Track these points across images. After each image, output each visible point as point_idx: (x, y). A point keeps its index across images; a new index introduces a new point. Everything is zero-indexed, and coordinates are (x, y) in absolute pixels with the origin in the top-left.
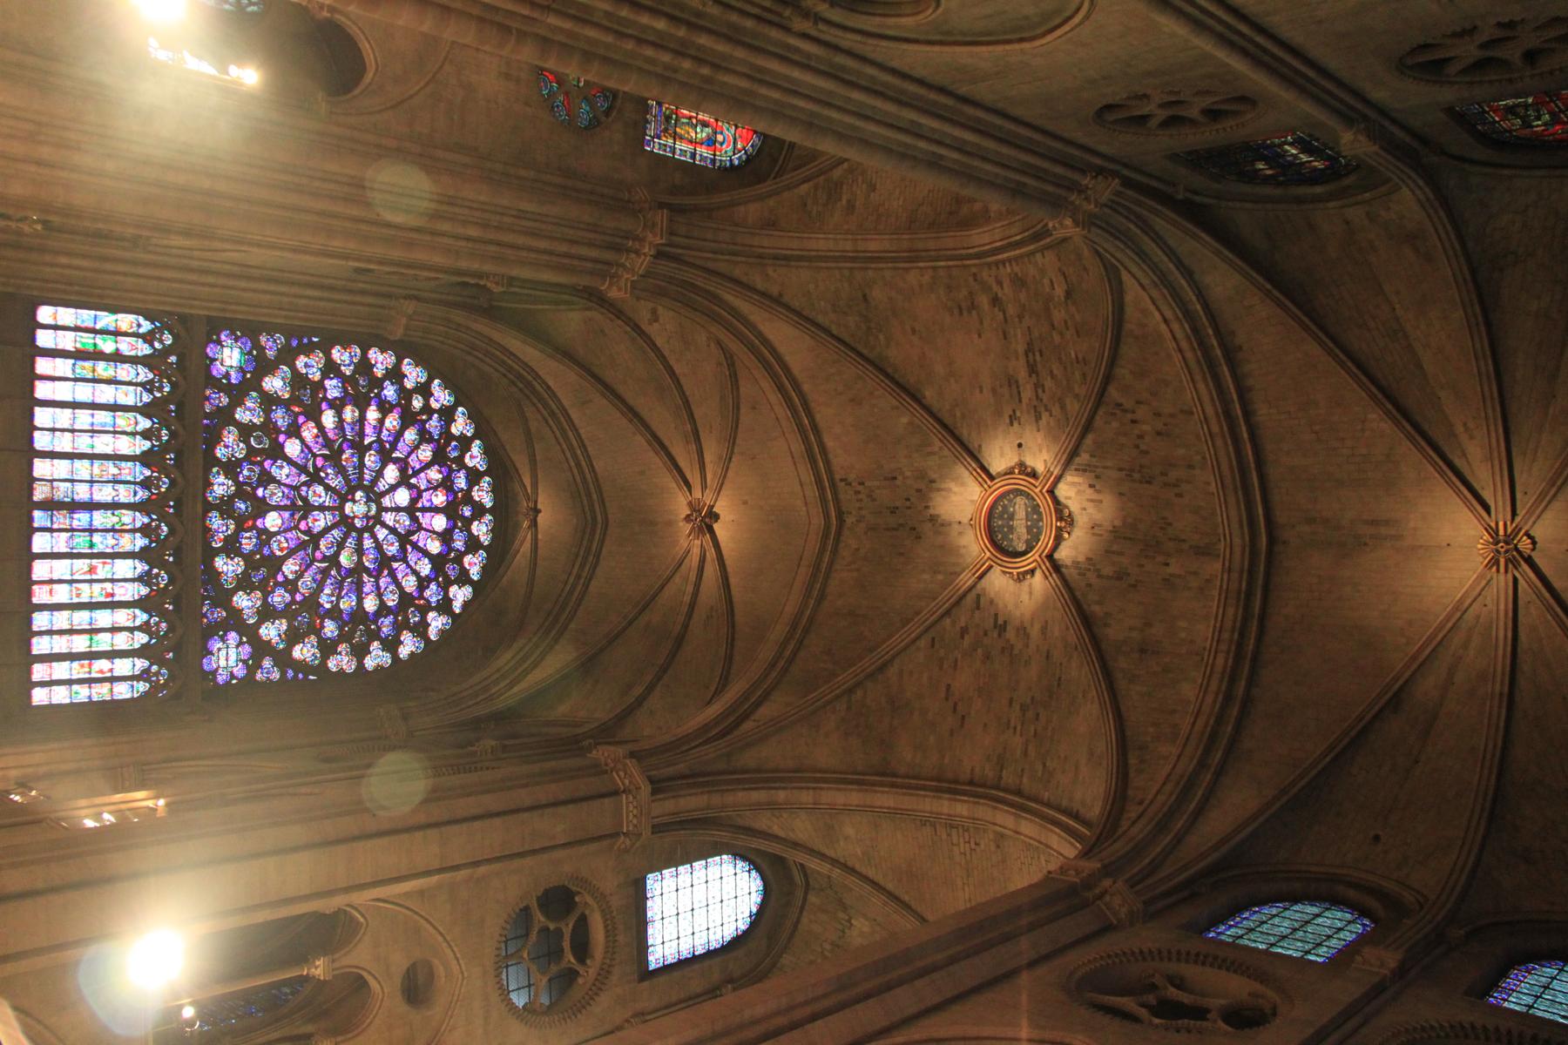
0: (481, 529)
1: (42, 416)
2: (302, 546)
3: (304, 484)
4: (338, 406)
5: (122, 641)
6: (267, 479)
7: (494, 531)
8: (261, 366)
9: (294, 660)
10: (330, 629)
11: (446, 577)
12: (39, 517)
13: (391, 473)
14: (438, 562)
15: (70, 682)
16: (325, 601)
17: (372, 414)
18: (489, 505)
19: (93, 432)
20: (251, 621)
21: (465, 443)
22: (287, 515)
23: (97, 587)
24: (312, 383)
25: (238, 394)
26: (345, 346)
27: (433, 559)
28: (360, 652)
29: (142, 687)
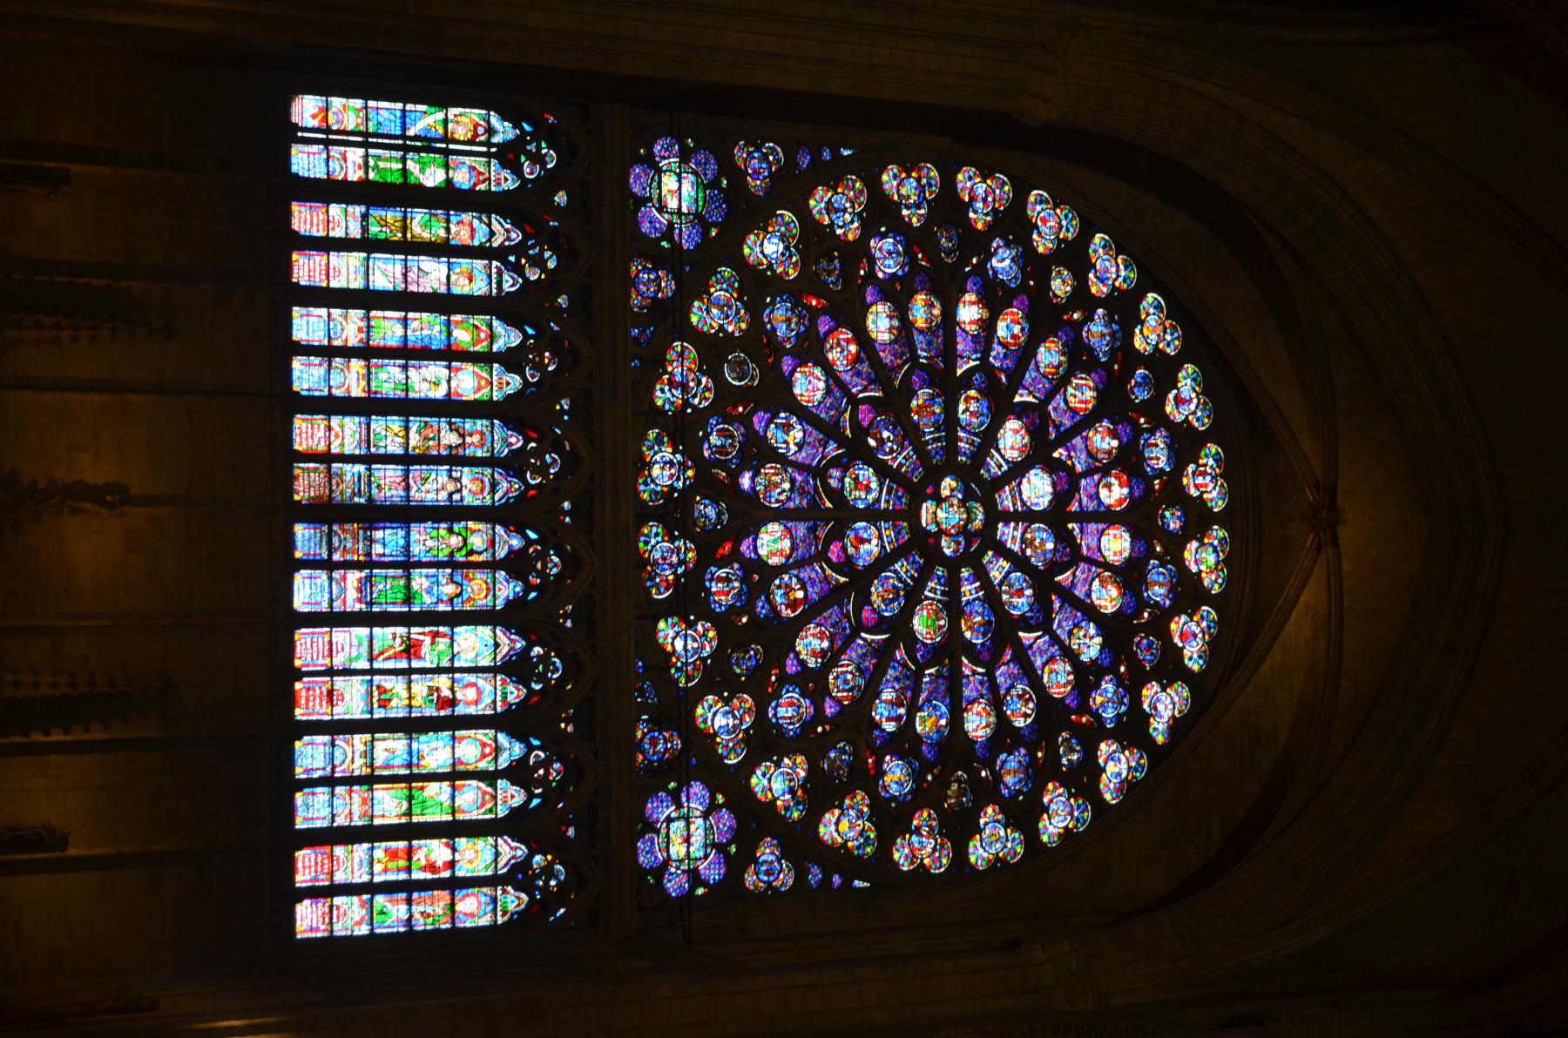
0: (1203, 559)
1: (308, 325)
2: (833, 595)
3: (835, 462)
4: (897, 294)
5: (470, 801)
6: (758, 453)
7: (1231, 562)
8: (738, 211)
10: (895, 776)
11: (1135, 664)
12: (305, 538)
13: (1012, 438)
14: (1114, 629)
15: (371, 888)
16: (885, 714)
17: (969, 313)
18: (1219, 506)
19: (408, 354)
21: (1163, 370)
22: (801, 529)
23: (420, 687)
24: (842, 243)
25: (693, 275)
26: (908, 166)
28: (959, 829)
29: (513, 900)
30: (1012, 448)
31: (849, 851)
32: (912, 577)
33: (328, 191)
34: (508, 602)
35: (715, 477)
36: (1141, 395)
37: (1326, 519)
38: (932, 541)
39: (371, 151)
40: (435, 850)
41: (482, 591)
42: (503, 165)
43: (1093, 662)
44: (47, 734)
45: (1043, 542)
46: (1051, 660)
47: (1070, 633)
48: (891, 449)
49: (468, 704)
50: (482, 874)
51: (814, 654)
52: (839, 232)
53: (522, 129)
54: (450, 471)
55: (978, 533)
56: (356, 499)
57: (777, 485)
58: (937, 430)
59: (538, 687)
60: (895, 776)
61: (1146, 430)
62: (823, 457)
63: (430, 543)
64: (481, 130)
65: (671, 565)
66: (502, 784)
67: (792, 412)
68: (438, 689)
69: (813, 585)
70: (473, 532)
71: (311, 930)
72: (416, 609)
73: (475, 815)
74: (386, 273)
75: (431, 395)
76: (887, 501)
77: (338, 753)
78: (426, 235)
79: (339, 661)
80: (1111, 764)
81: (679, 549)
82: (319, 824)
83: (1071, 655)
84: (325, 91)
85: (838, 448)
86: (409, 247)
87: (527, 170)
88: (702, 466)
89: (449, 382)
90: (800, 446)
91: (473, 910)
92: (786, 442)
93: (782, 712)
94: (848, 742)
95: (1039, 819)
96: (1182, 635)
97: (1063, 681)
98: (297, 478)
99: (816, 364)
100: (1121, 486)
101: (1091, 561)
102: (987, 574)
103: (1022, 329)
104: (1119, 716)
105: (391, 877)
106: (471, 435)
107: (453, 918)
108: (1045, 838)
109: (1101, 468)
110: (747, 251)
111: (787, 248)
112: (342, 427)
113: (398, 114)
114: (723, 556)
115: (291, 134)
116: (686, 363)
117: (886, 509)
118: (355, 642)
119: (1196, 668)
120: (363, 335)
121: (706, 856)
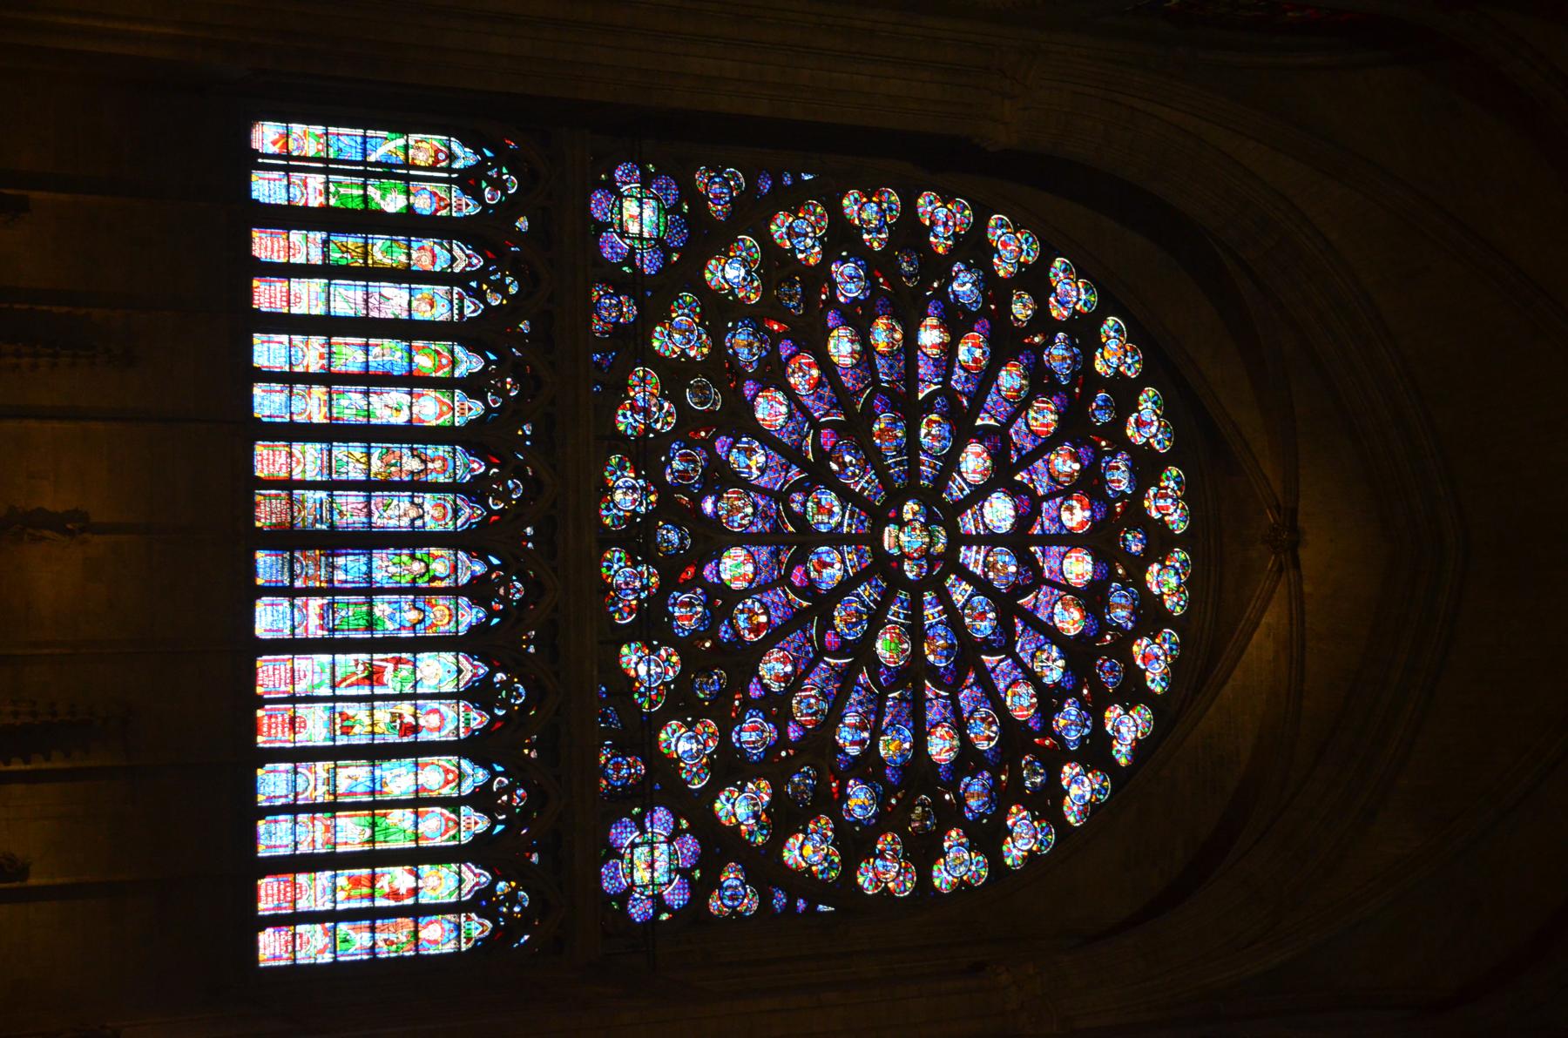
0: (1164, 581)
1: (268, 352)
2: (797, 619)
3: (797, 486)
4: (859, 319)
5: (434, 827)
6: (721, 478)
8: (700, 236)
9: (785, 865)
10: (859, 799)
12: (267, 565)
13: (974, 462)
14: (1077, 651)
15: (334, 916)
16: (847, 737)
17: (930, 337)
18: (1180, 528)
20: (697, 785)
21: (1124, 393)
22: (764, 554)
23: (383, 713)
24: (804, 268)
27: (1069, 647)
28: (923, 852)
29: (476, 927)
30: (974, 471)
31: (813, 875)
32: (875, 601)
33: (289, 217)
34: (471, 628)
35: (678, 502)
36: (1103, 418)
37: (1287, 541)
38: (894, 564)
39: (332, 177)
40: (398, 878)
41: (442, 617)
42: (465, 191)
43: (1056, 684)
44: (7, 763)
45: (1005, 565)
46: (1014, 683)
47: (1033, 656)
48: (854, 475)
49: (431, 730)
50: (446, 900)
51: (778, 679)
52: (800, 256)
53: (483, 155)
54: (412, 497)
55: (940, 556)
56: (318, 526)
57: (739, 510)
58: (900, 453)
59: (501, 713)
60: (859, 799)
61: (1107, 453)
62: (786, 482)
63: (392, 569)
64: (442, 156)
65: (634, 590)
66: (465, 810)
67: (755, 437)
68: (401, 716)
69: (776, 609)
70: (436, 558)
71: (275, 958)
72: (378, 635)
73: (439, 842)
74: (347, 299)
75: (393, 421)
76: (850, 525)
77: (301, 780)
78: (387, 262)
79: (301, 688)
80: (1074, 786)
81: (641, 574)
82: (281, 852)
83: (1033, 678)
84: (284, 116)
85: (800, 472)
86: (370, 274)
87: (487, 195)
88: (665, 490)
89: (410, 408)
90: (762, 470)
91: (437, 937)
92: (748, 467)
93: (745, 736)
94: (812, 766)
95: (1003, 842)
96: (1144, 658)
97: (1026, 704)
98: (257, 504)
99: (778, 389)
100: (1083, 509)
101: (1053, 584)
102: (950, 597)
103: (984, 353)
104: (1082, 739)
105: (354, 904)
106: (433, 461)
107: (417, 945)
108: (1009, 861)
109: (1063, 491)
110: (708, 276)
111: (748, 273)
112: (303, 453)
113: (359, 140)
114: (686, 581)
115: (252, 160)
116: (649, 388)
117: (849, 533)
118: (317, 669)
119: (1158, 690)
120: (325, 362)
121: (670, 882)
